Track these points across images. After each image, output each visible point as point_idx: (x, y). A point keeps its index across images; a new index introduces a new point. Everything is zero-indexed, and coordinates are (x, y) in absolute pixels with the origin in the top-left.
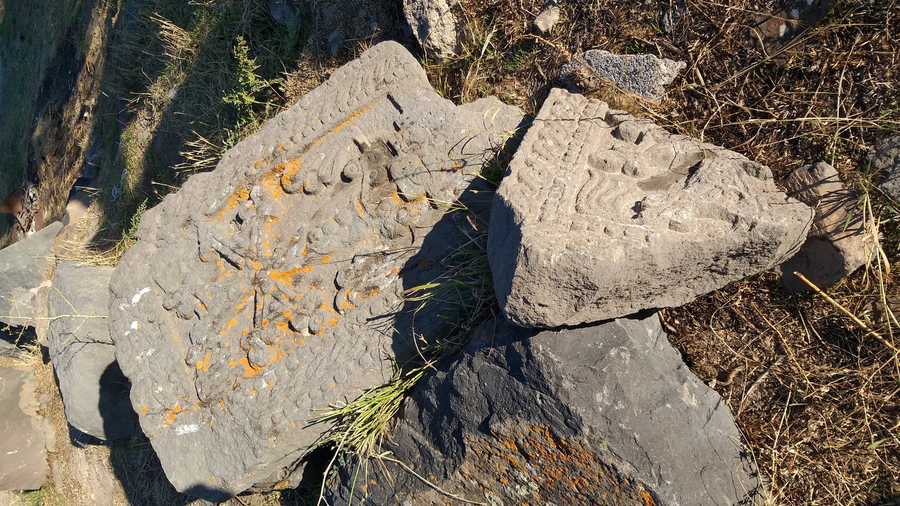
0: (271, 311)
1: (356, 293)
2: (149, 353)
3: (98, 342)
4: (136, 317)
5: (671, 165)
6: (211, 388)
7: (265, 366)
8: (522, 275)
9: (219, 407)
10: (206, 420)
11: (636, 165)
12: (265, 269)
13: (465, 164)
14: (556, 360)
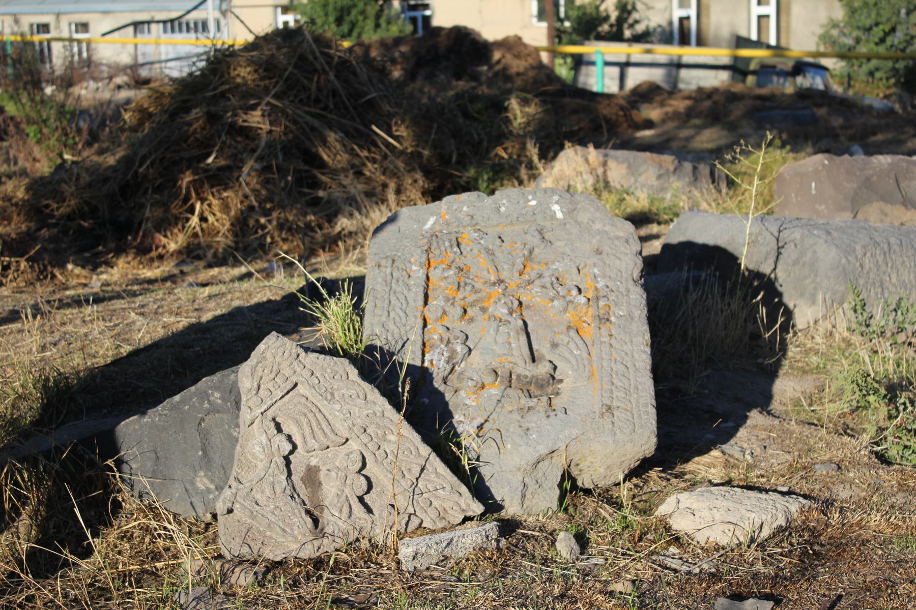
3: (779, 254)
4: (539, 204)
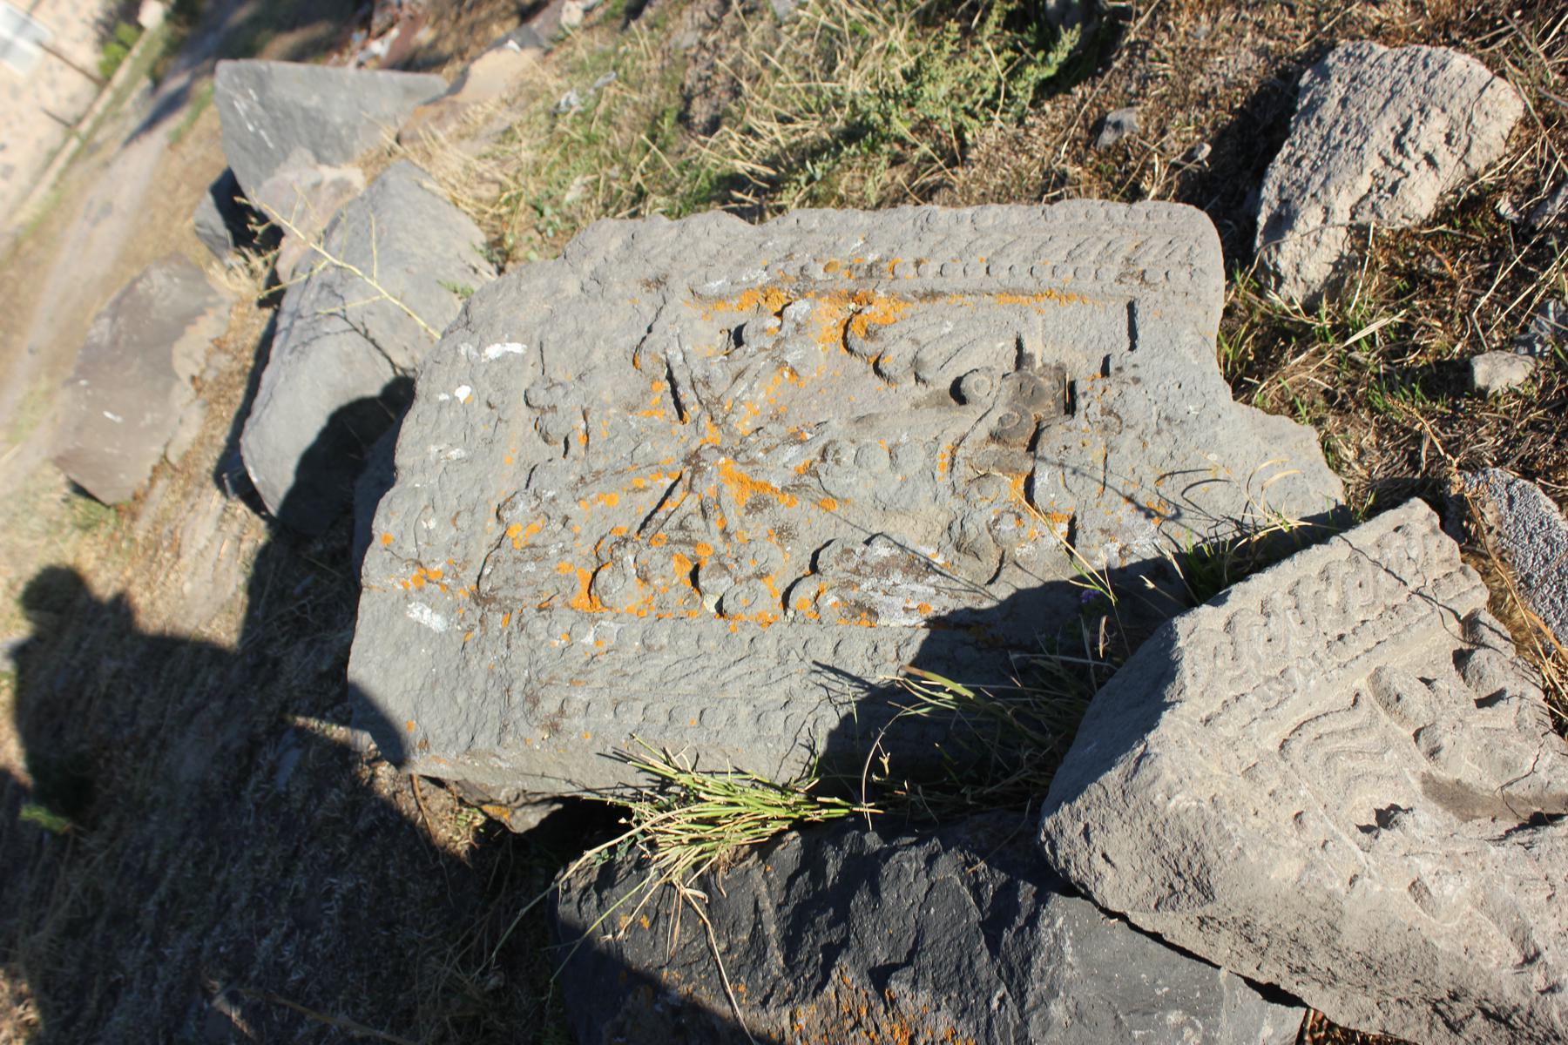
0: (681, 527)
1: (835, 599)
2: (455, 453)
3: (373, 341)
4: (472, 381)
5: (1510, 784)
6: (506, 581)
7: (611, 608)
8: (1110, 790)
9: (497, 620)
10: (464, 625)
11: (1445, 741)
12: (722, 451)
13: (1178, 515)
14: (1069, 959)
